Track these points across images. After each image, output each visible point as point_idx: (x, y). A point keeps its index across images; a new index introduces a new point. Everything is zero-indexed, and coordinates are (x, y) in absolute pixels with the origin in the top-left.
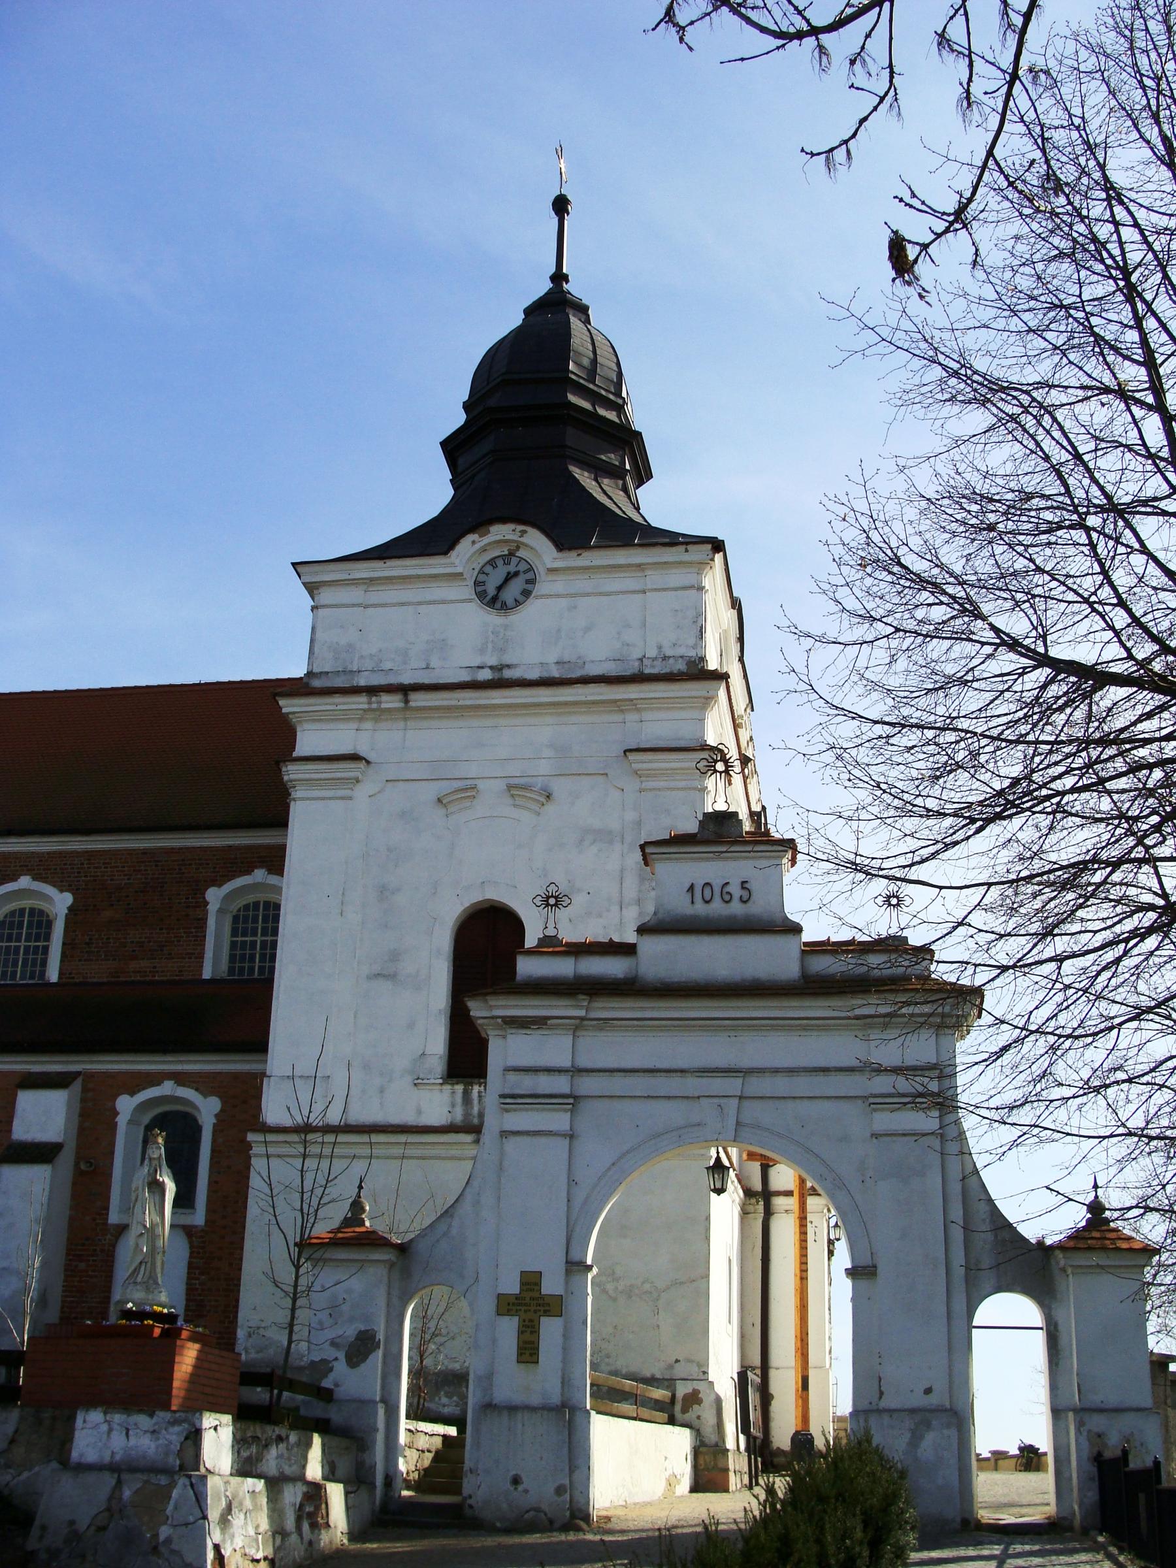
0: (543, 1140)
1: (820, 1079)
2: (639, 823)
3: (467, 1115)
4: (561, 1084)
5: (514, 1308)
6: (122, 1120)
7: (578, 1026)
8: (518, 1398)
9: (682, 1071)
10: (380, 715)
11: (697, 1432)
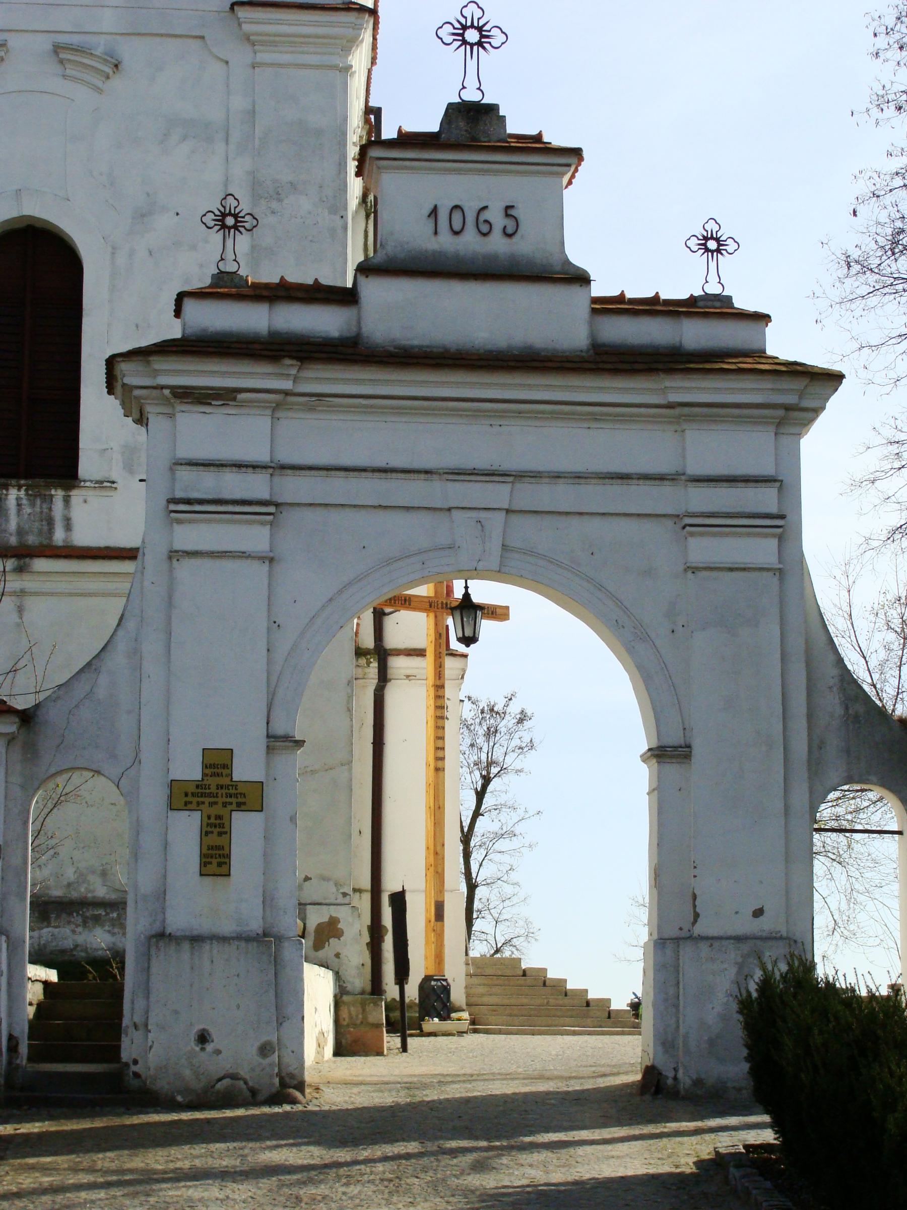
0: (228, 565)
1: (616, 489)
2: (252, 113)
4: (256, 486)
5: (195, 800)
7: (280, 403)
8: (204, 926)
9: (427, 472)
11: (338, 976)
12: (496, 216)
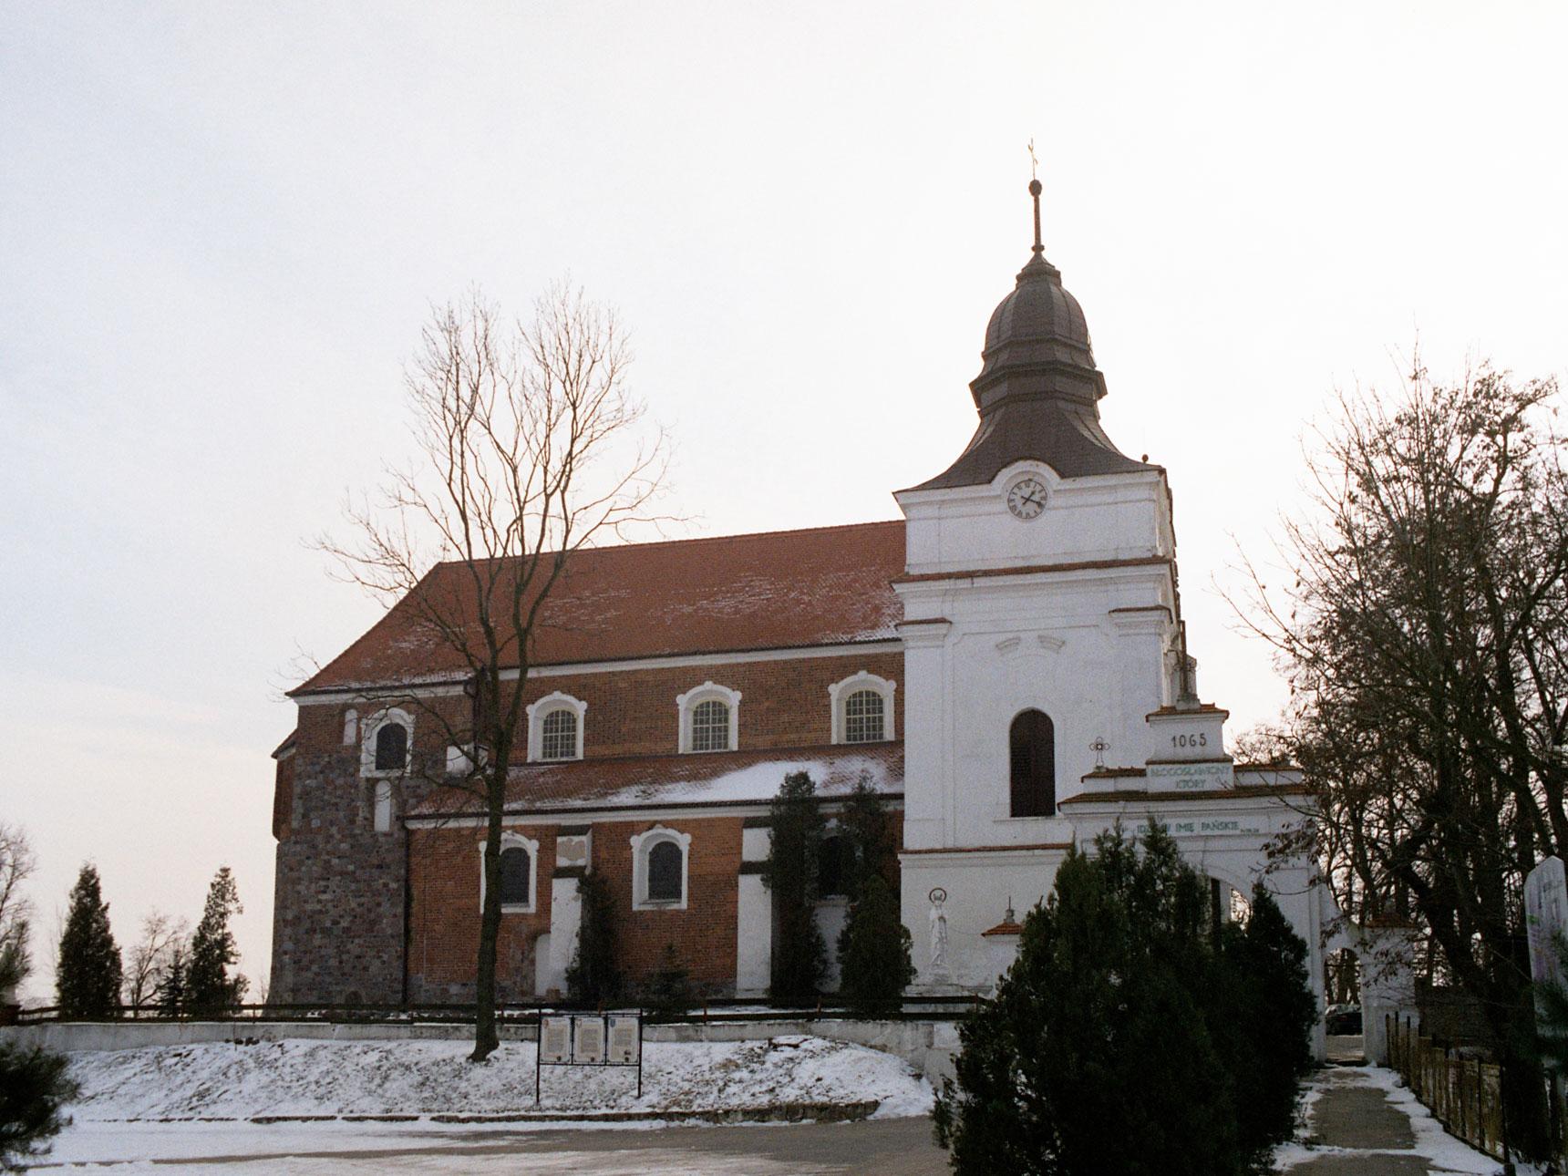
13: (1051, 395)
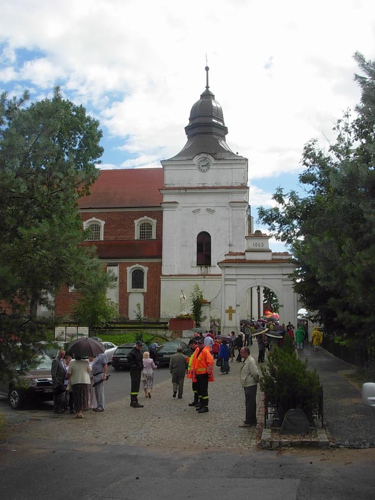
3: (201, 272)
4: (234, 277)
6: (128, 272)
7: (236, 267)
10: (180, 194)
12: (261, 244)
13: (212, 133)
